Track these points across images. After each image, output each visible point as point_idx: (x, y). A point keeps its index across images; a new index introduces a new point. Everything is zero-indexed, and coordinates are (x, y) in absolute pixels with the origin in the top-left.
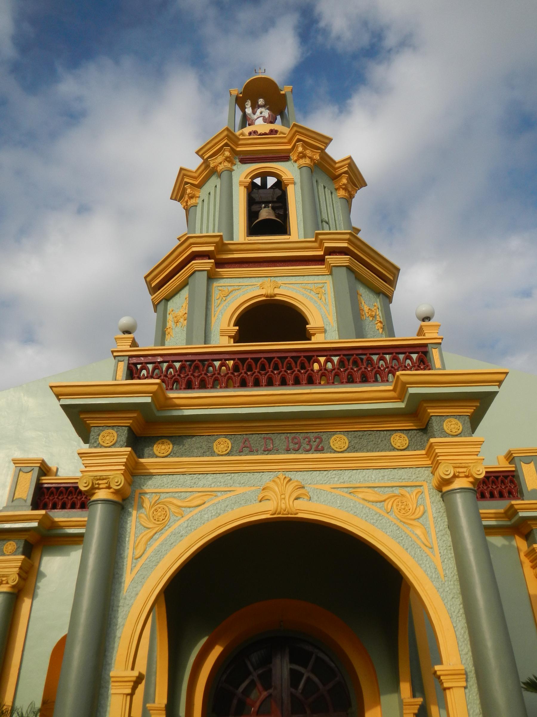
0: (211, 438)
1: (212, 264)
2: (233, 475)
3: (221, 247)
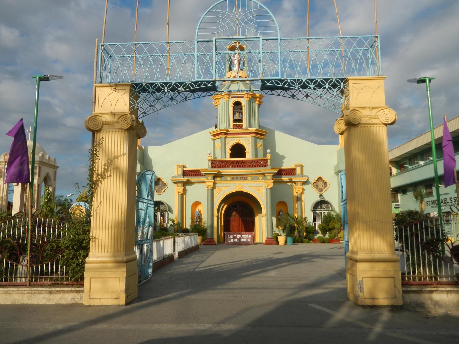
3: (228, 131)
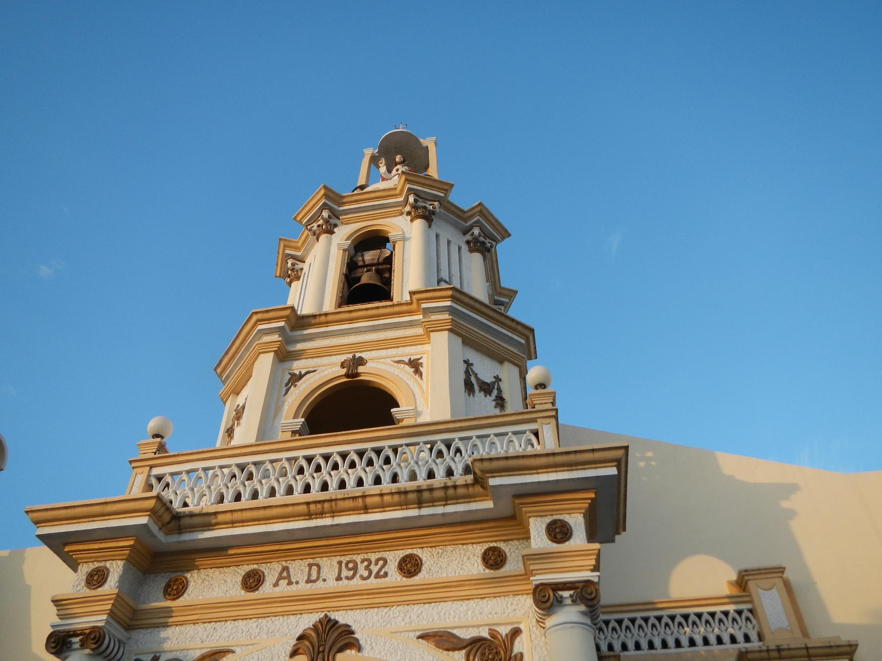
0: (239, 571)
1: (279, 343)
2: (260, 620)
